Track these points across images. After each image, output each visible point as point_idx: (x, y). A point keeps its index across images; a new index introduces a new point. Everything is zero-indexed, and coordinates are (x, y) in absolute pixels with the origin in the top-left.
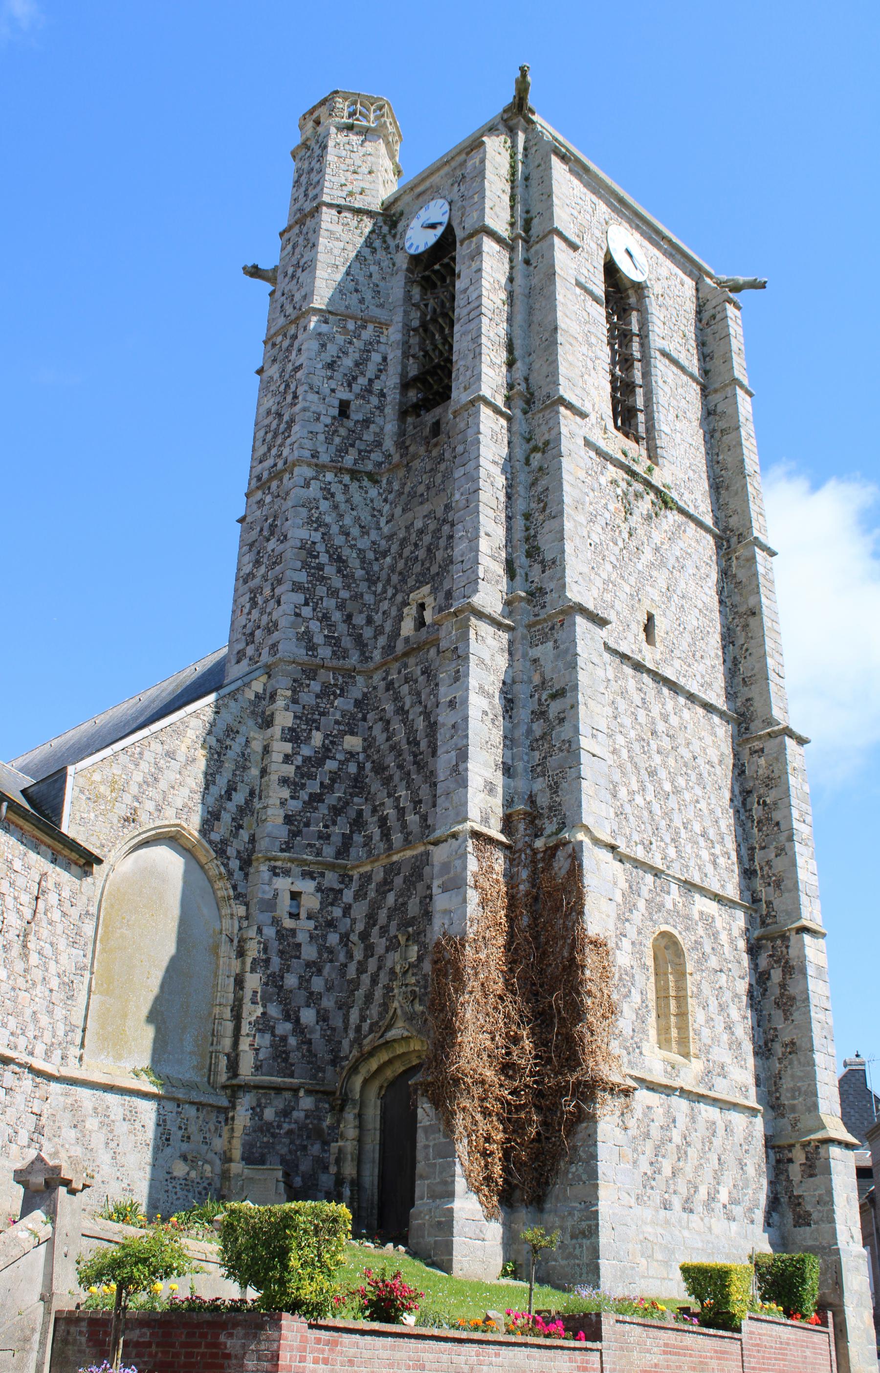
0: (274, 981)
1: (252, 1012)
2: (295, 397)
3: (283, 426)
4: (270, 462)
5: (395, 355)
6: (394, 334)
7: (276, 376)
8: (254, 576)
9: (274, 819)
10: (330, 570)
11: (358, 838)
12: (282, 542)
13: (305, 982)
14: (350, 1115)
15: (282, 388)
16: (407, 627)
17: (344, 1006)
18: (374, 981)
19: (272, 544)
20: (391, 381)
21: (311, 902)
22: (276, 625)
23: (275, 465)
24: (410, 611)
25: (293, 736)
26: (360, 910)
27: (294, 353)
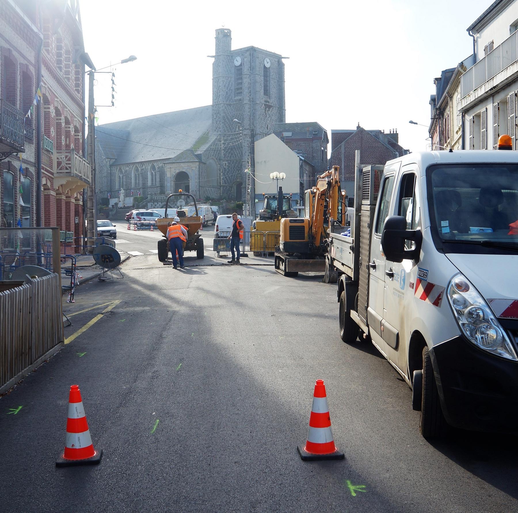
0: (224, 174)
1: (222, 178)
5: (233, 83)
6: (233, 79)
9: (222, 154)
10: (227, 120)
13: (227, 174)
16: (237, 129)
20: (233, 88)
21: (227, 164)
24: (237, 127)
25: (224, 144)
26: (233, 165)
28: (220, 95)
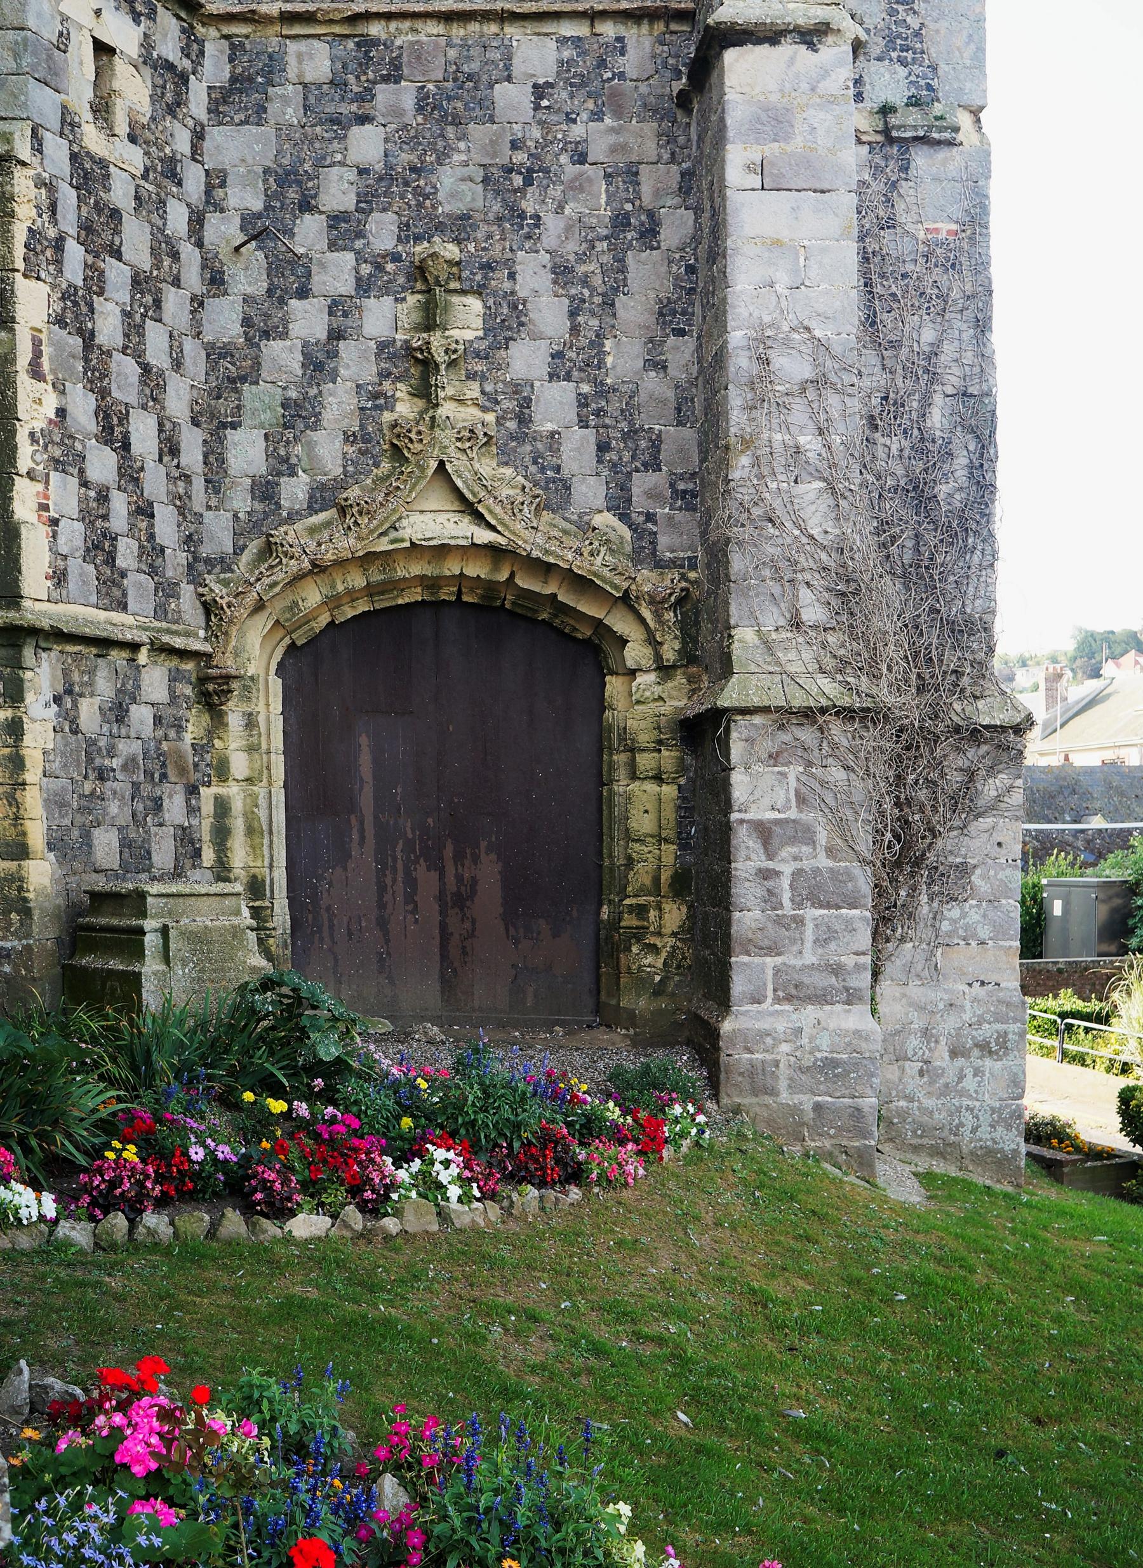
14: (234, 720)
17: (216, 423)
18: (319, 364)
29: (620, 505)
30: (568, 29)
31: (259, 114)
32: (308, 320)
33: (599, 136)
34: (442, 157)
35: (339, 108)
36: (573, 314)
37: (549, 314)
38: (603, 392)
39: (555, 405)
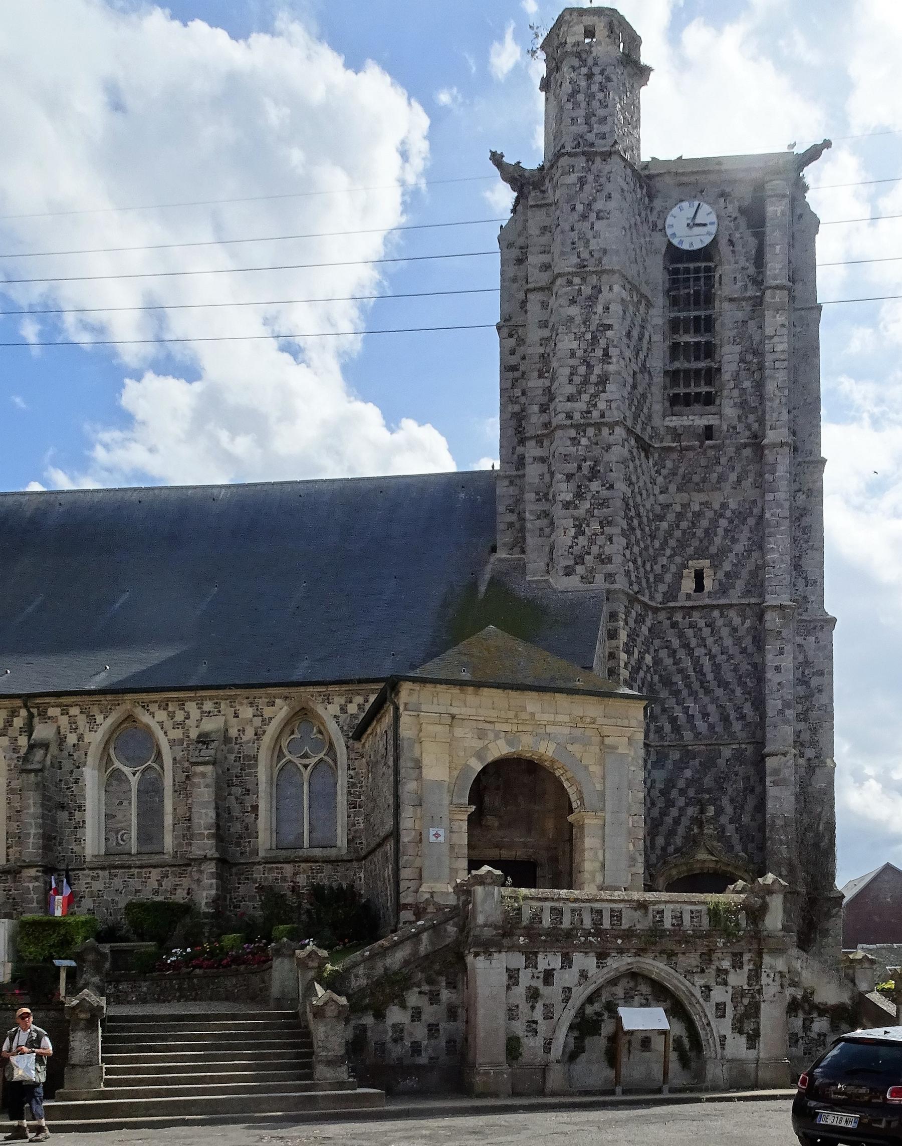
2: (606, 354)
3: (593, 379)
4: (581, 406)
7: (578, 320)
8: (576, 507)
11: (652, 726)
12: (608, 489)
15: (588, 336)
19: (595, 486)
22: (610, 560)
23: (589, 412)
27: (599, 309)
28: (603, 380)
29: (745, 850)
30: (734, 747)
31: (663, 767)
32: (674, 812)
33: (741, 769)
34: (705, 776)
35: (680, 766)
36: (735, 809)
37: (729, 809)
38: (741, 826)
39: (730, 829)
